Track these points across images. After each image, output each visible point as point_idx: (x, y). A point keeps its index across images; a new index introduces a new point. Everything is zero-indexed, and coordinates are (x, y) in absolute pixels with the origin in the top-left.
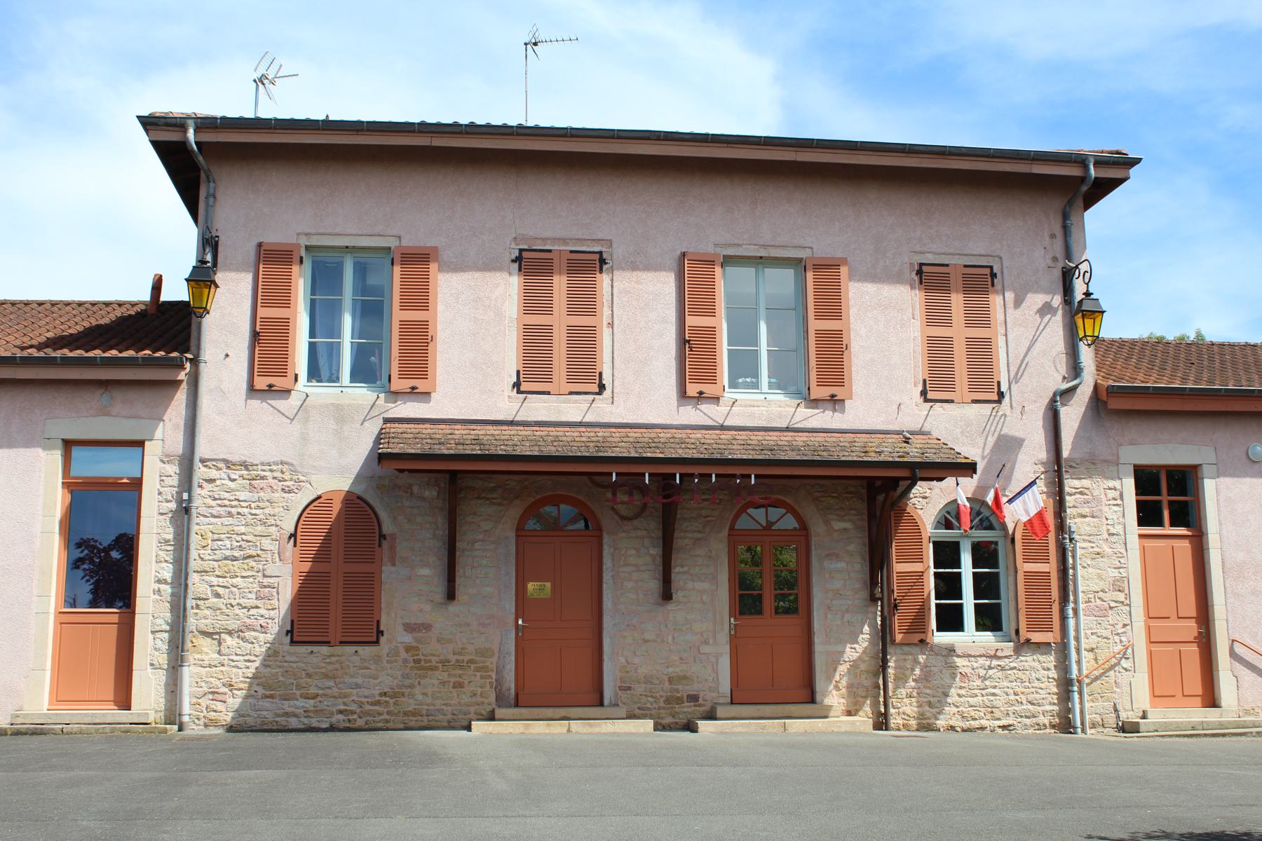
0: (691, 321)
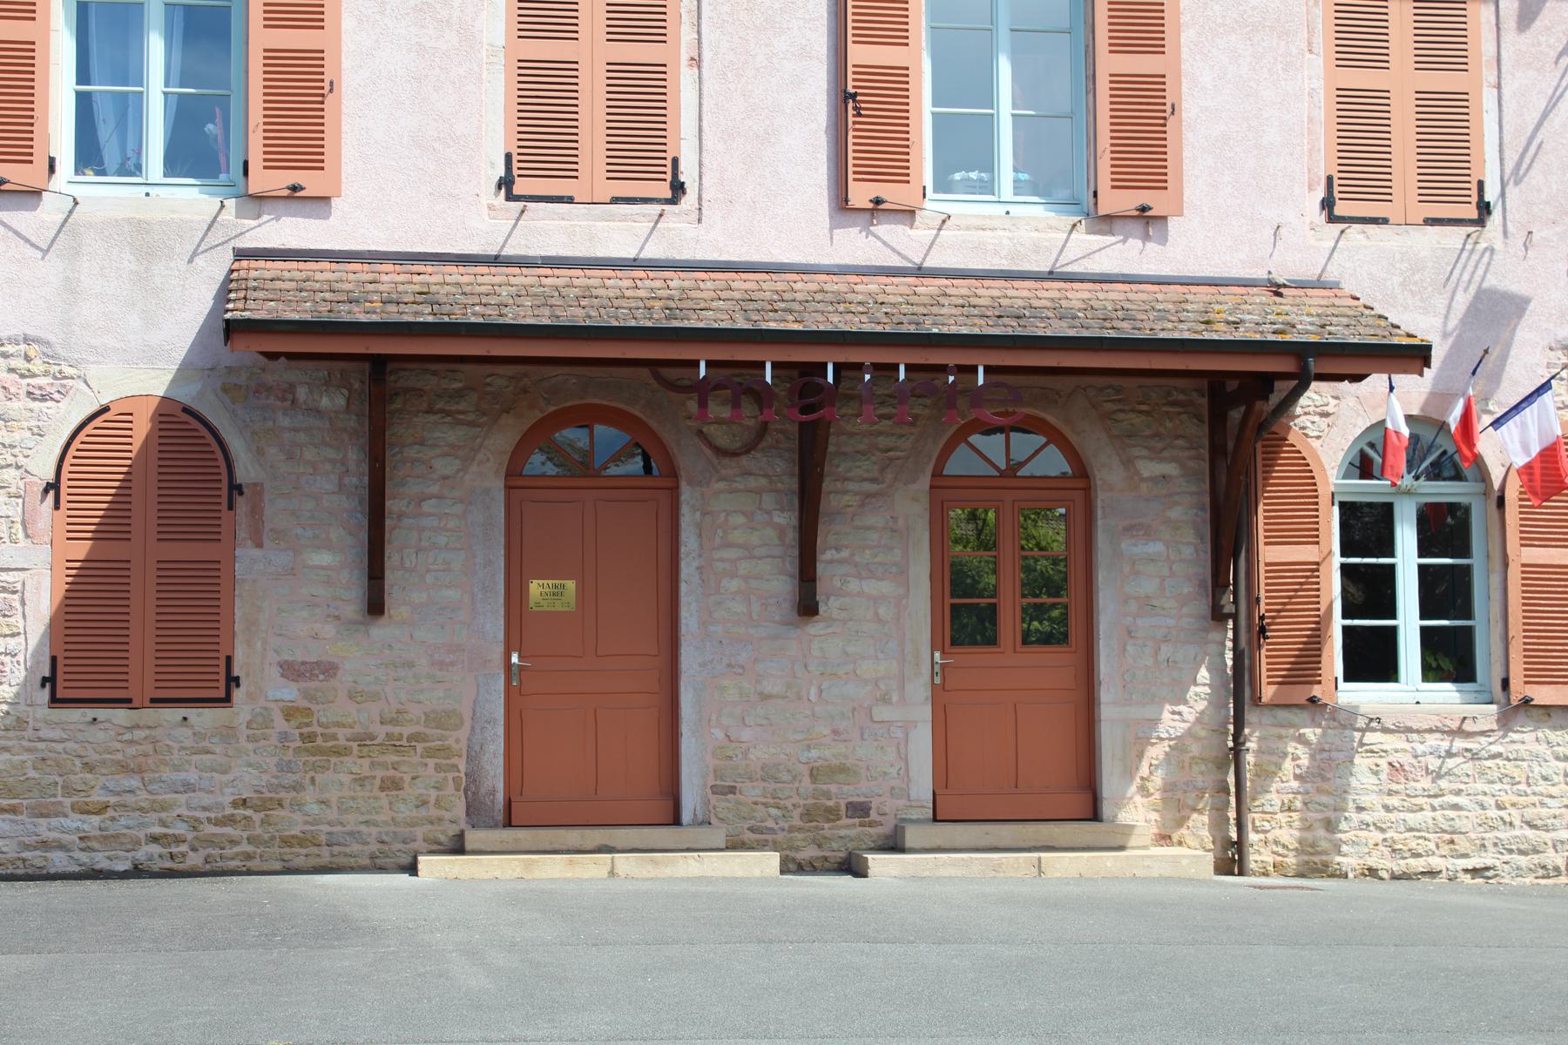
0: (859, 54)
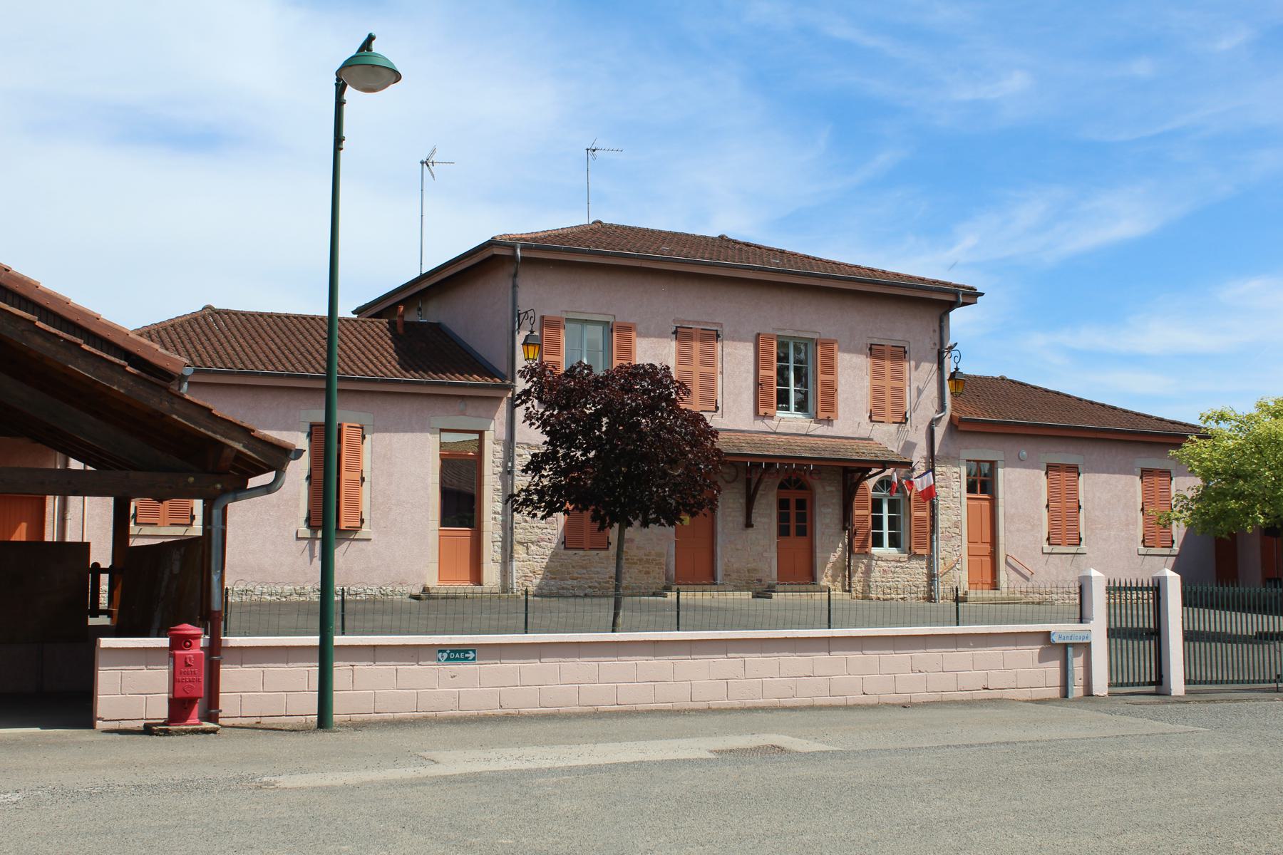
0: (762, 372)
